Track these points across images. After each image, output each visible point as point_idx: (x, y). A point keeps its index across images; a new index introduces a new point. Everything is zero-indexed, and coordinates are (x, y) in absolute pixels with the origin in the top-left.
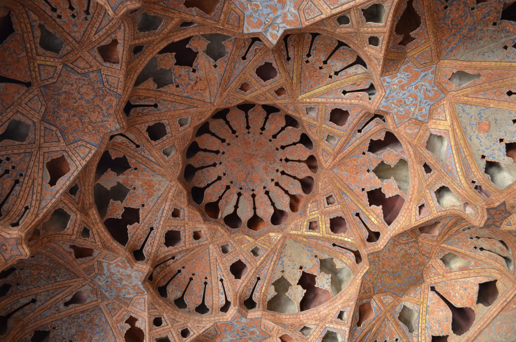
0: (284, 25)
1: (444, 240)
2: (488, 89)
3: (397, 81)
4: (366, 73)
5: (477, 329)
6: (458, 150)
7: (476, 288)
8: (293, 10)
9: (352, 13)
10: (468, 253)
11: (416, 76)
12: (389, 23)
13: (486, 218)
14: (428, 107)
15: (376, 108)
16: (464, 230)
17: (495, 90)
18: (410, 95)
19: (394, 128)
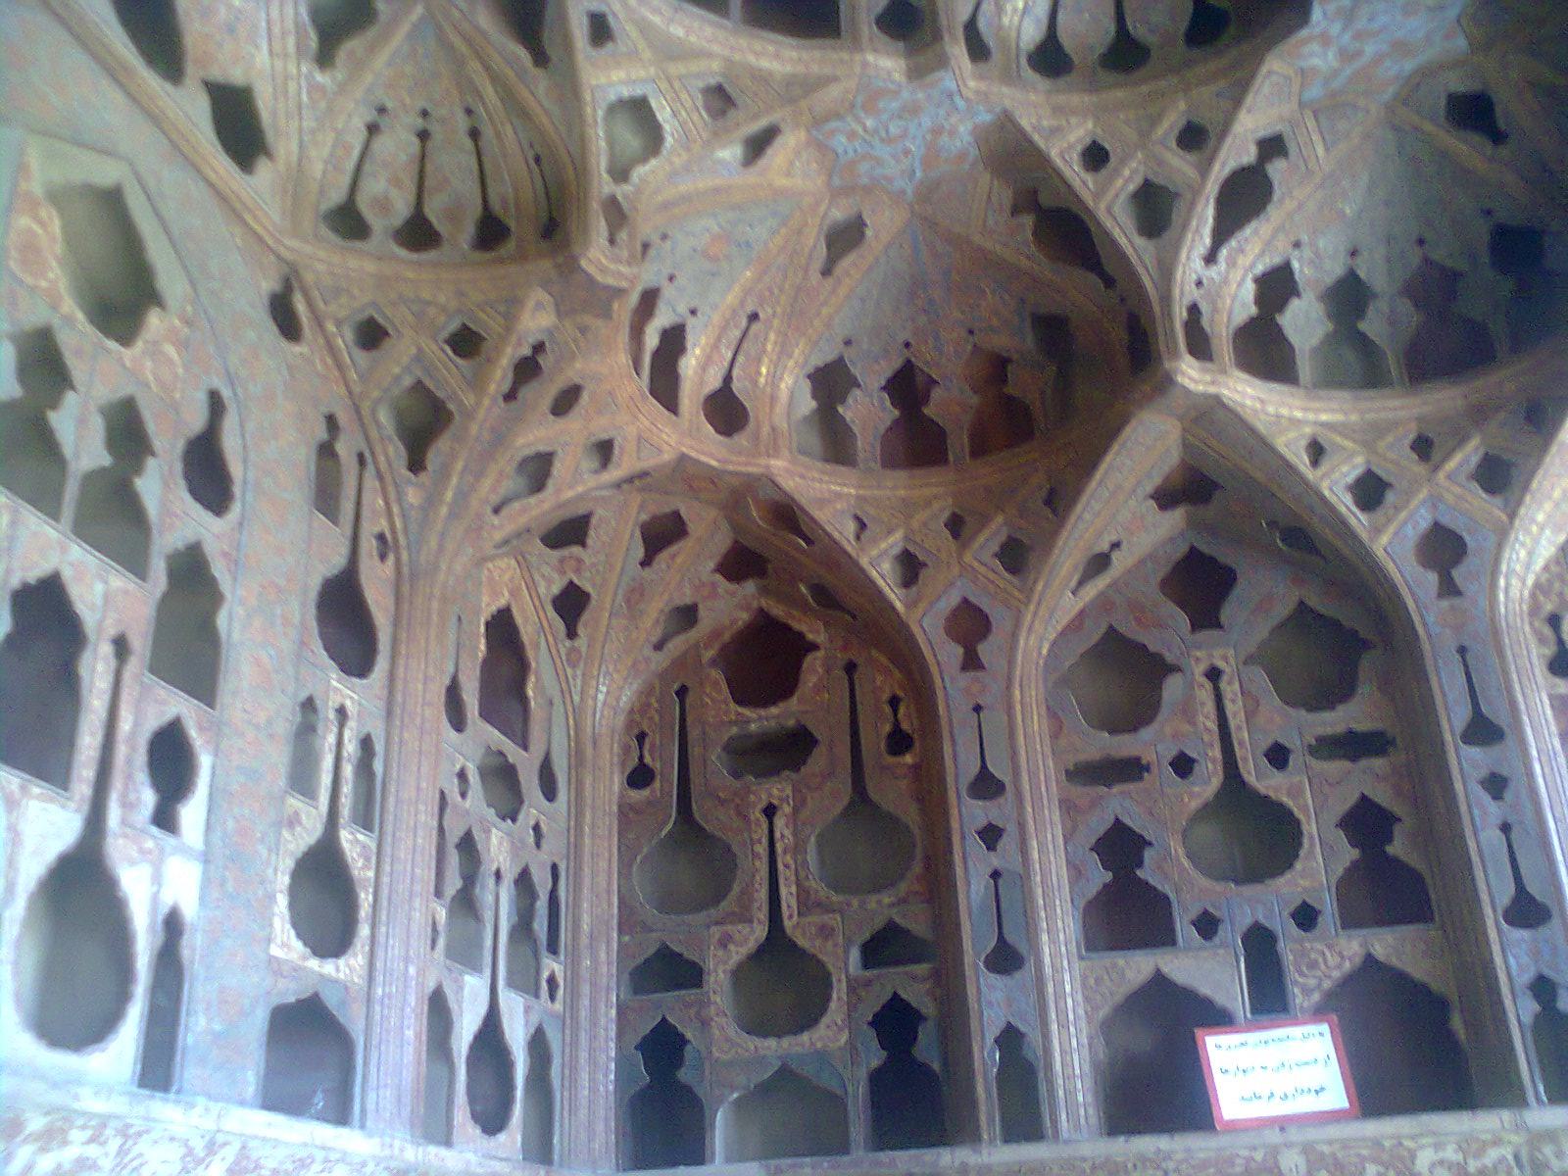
0: (1318, 30)
1: (448, 29)
2: (786, 277)
3: (962, 129)
4: (1018, 56)
5: (160, 103)
6: (717, 190)
7: (237, 76)
8: (1316, 61)
9: (1191, 173)
10: (369, 78)
11: (927, 162)
12: (1108, 223)
13: (599, 278)
14: (840, 150)
15: (953, 62)
16: (469, 112)
17: (776, 291)
18: (904, 135)
19: (865, 64)
